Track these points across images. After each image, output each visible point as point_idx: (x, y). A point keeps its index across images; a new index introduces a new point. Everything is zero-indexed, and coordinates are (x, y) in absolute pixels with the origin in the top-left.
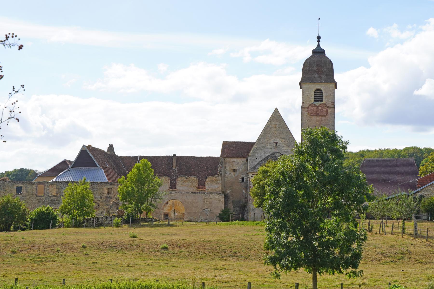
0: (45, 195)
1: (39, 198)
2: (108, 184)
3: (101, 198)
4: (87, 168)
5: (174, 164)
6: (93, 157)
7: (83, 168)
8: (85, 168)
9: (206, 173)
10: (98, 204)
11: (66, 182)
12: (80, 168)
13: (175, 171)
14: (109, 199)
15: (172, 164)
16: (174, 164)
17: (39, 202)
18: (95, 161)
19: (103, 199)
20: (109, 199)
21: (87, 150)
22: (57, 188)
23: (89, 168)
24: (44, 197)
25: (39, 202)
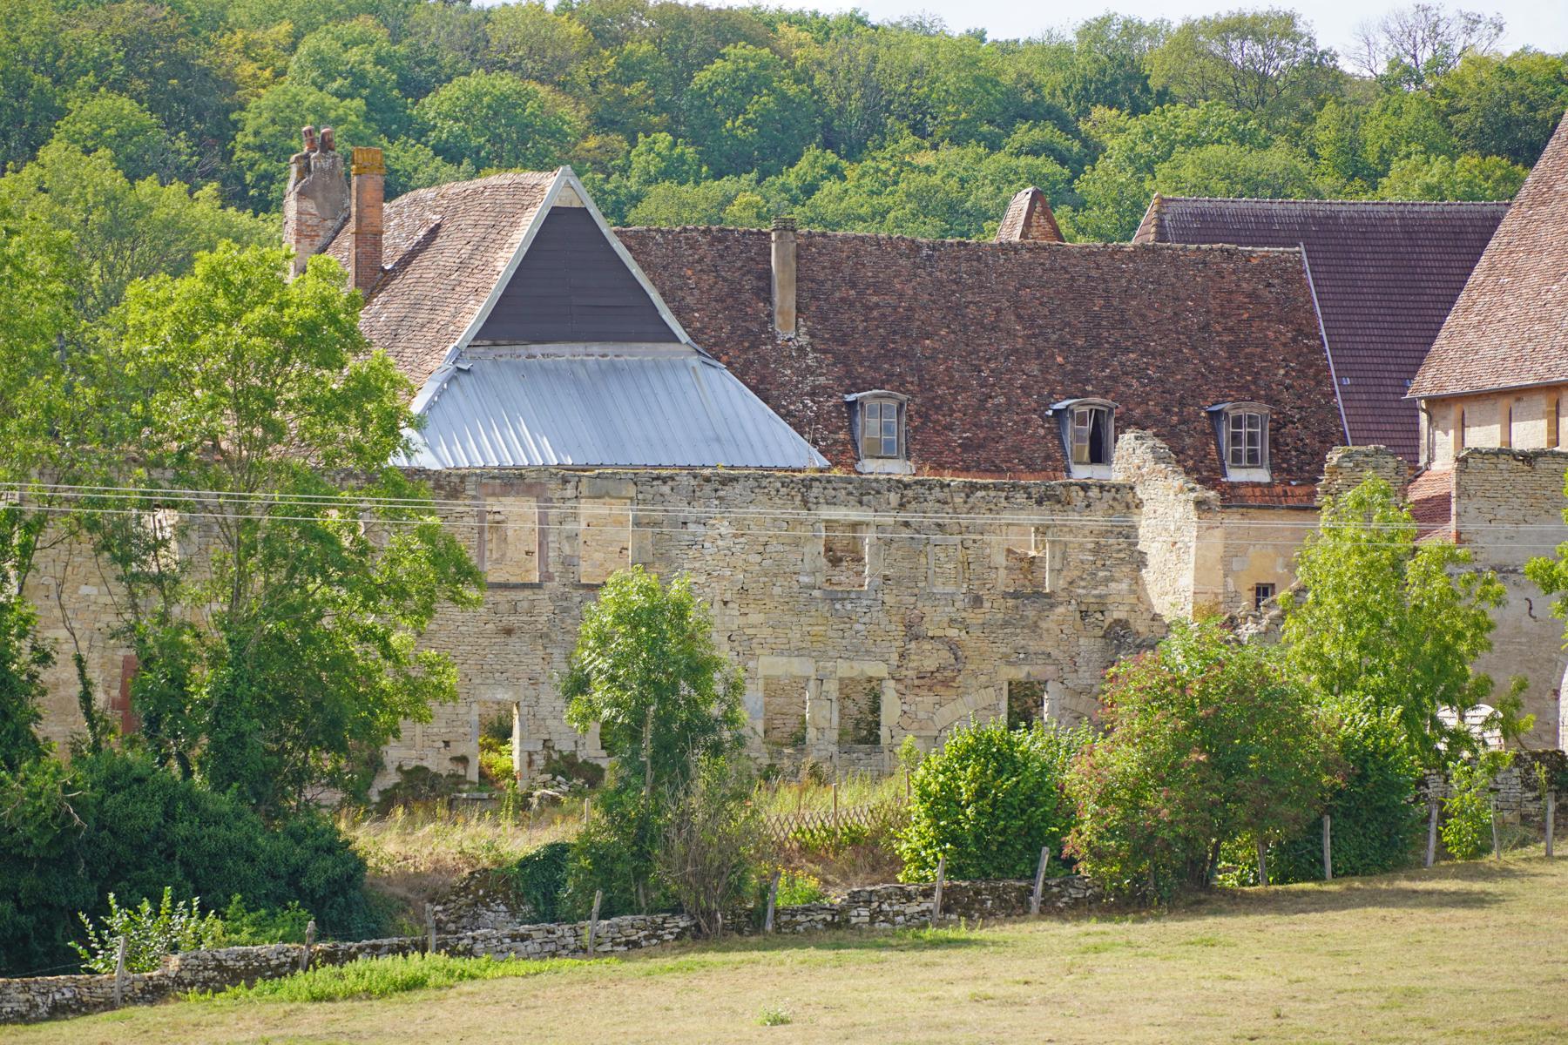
0: (550, 578)
1: (502, 597)
2: (1020, 497)
3: (977, 601)
4: (596, 348)
5: (784, 297)
6: (635, 270)
7: (565, 352)
8: (579, 348)
9: (1034, 368)
10: (953, 647)
11: (708, 480)
12: (536, 349)
13: (801, 349)
14: (1031, 613)
15: (765, 293)
16: (784, 297)
17: (509, 632)
18: (654, 296)
19: (994, 609)
20: (1031, 613)
21: (594, 211)
22: (637, 524)
23: (611, 349)
24: (542, 595)
25: (509, 632)
